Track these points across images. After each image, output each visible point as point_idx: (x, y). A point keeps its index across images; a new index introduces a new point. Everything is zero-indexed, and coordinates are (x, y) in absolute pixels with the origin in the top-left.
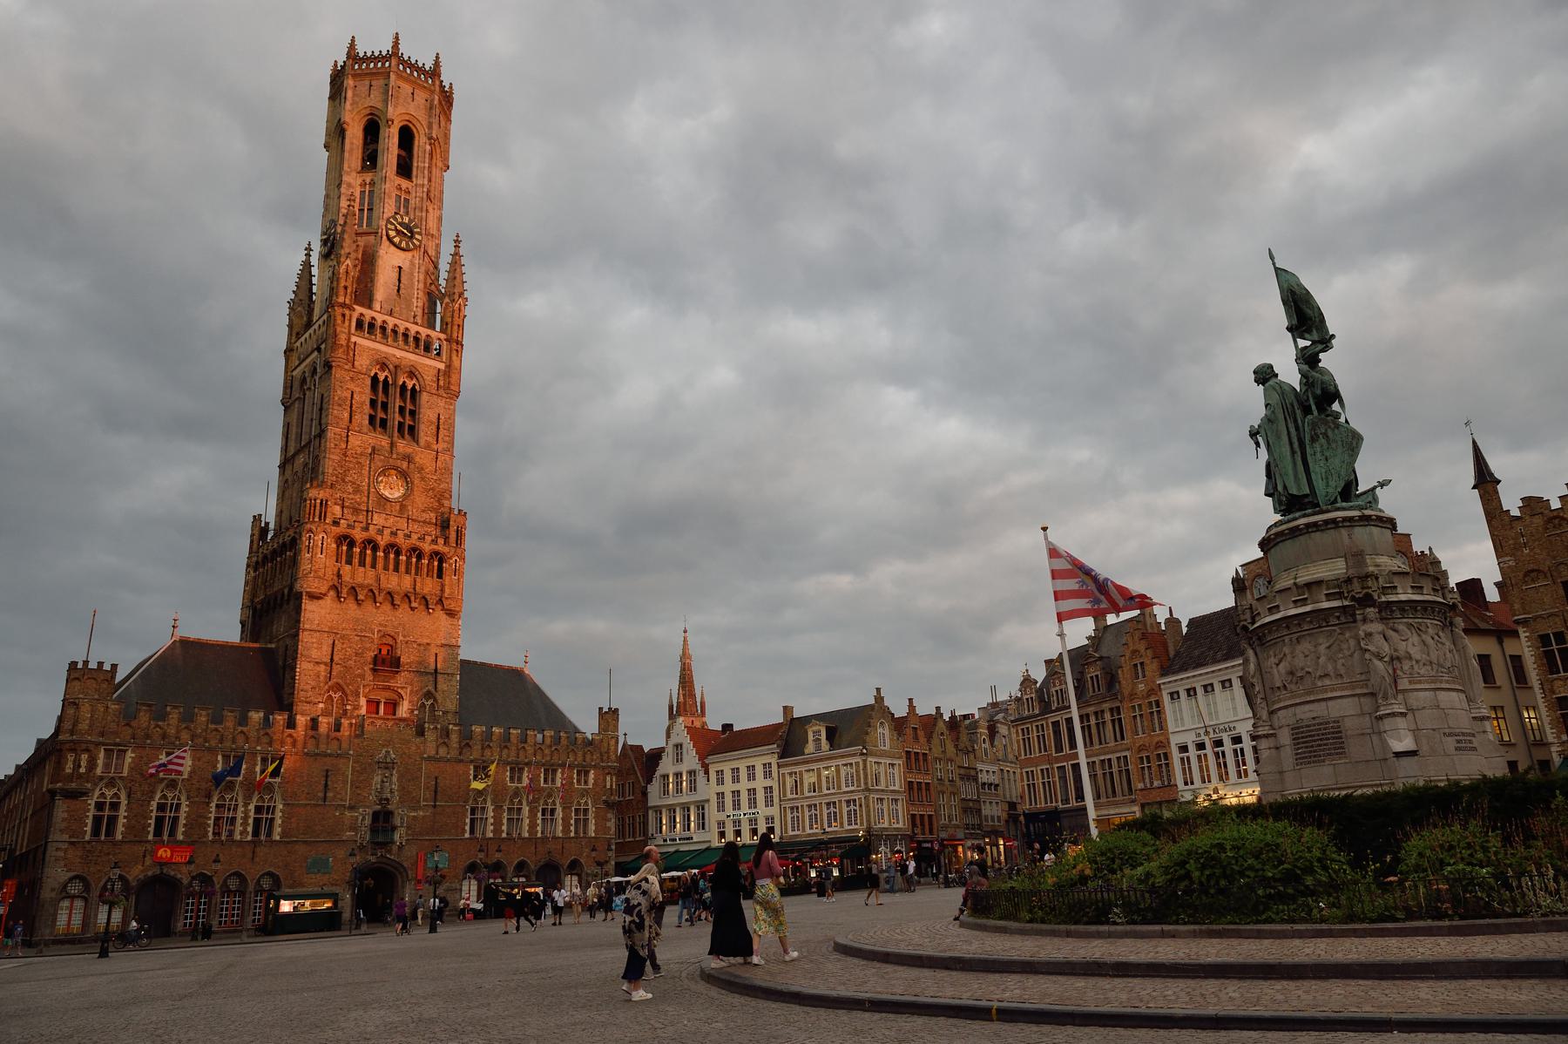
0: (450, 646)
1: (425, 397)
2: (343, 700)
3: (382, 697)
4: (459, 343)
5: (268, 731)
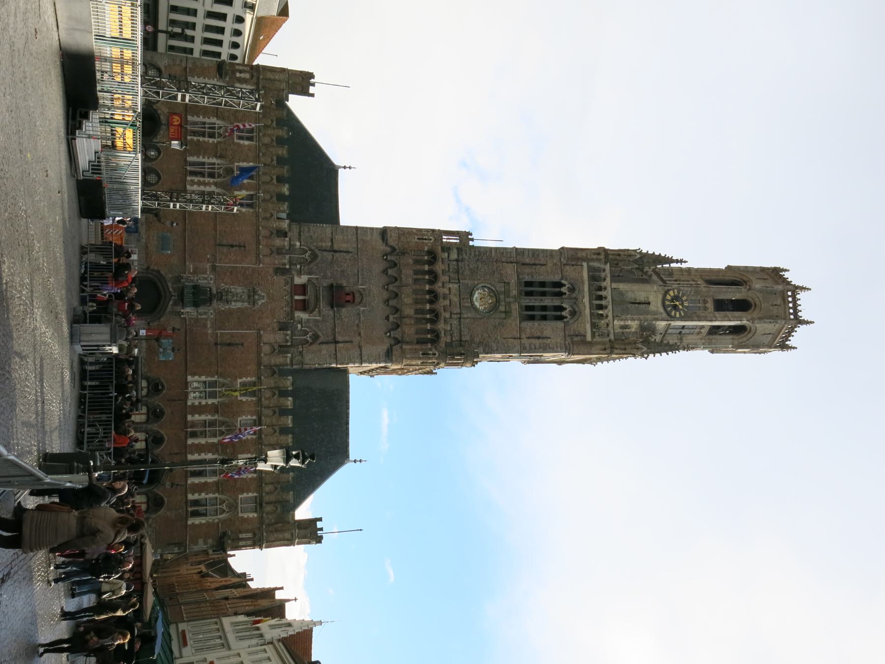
0: (361, 355)
1: (560, 324)
2: (304, 263)
3: (310, 295)
5: (274, 199)
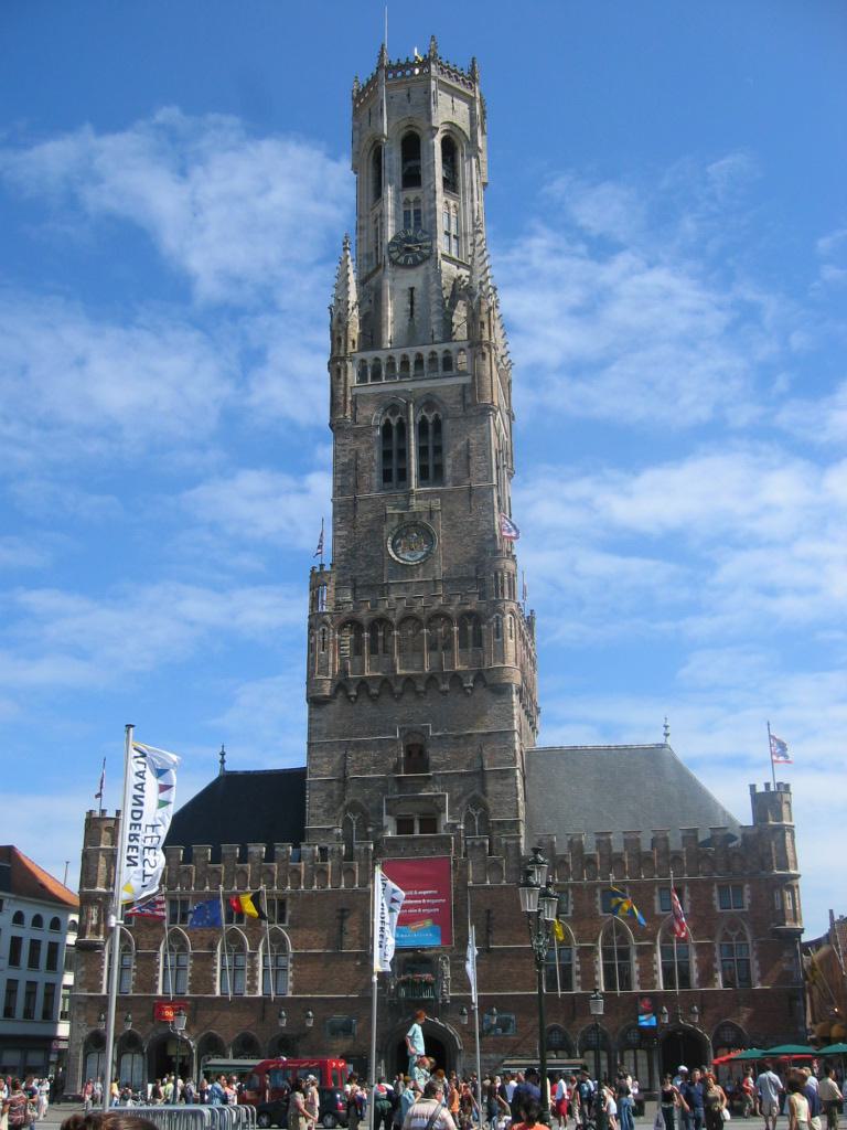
1: (447, 425)
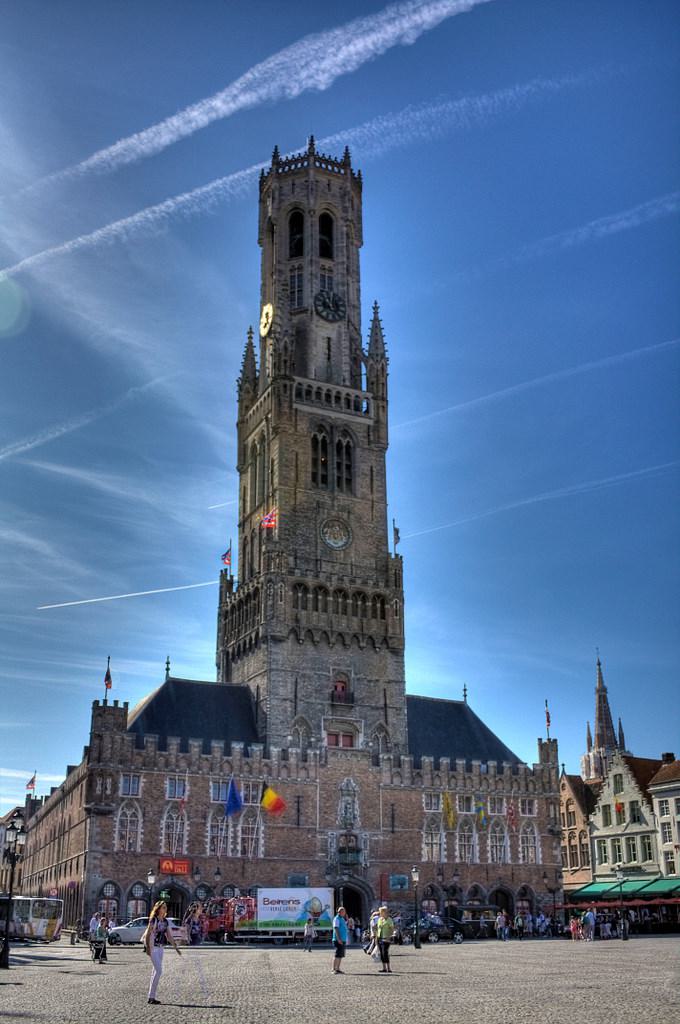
0: (396, 682)
1: (358, 451)
4: (384, 399)
5: (249, 760)
